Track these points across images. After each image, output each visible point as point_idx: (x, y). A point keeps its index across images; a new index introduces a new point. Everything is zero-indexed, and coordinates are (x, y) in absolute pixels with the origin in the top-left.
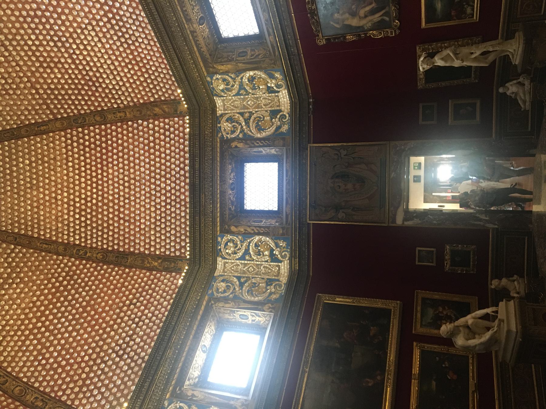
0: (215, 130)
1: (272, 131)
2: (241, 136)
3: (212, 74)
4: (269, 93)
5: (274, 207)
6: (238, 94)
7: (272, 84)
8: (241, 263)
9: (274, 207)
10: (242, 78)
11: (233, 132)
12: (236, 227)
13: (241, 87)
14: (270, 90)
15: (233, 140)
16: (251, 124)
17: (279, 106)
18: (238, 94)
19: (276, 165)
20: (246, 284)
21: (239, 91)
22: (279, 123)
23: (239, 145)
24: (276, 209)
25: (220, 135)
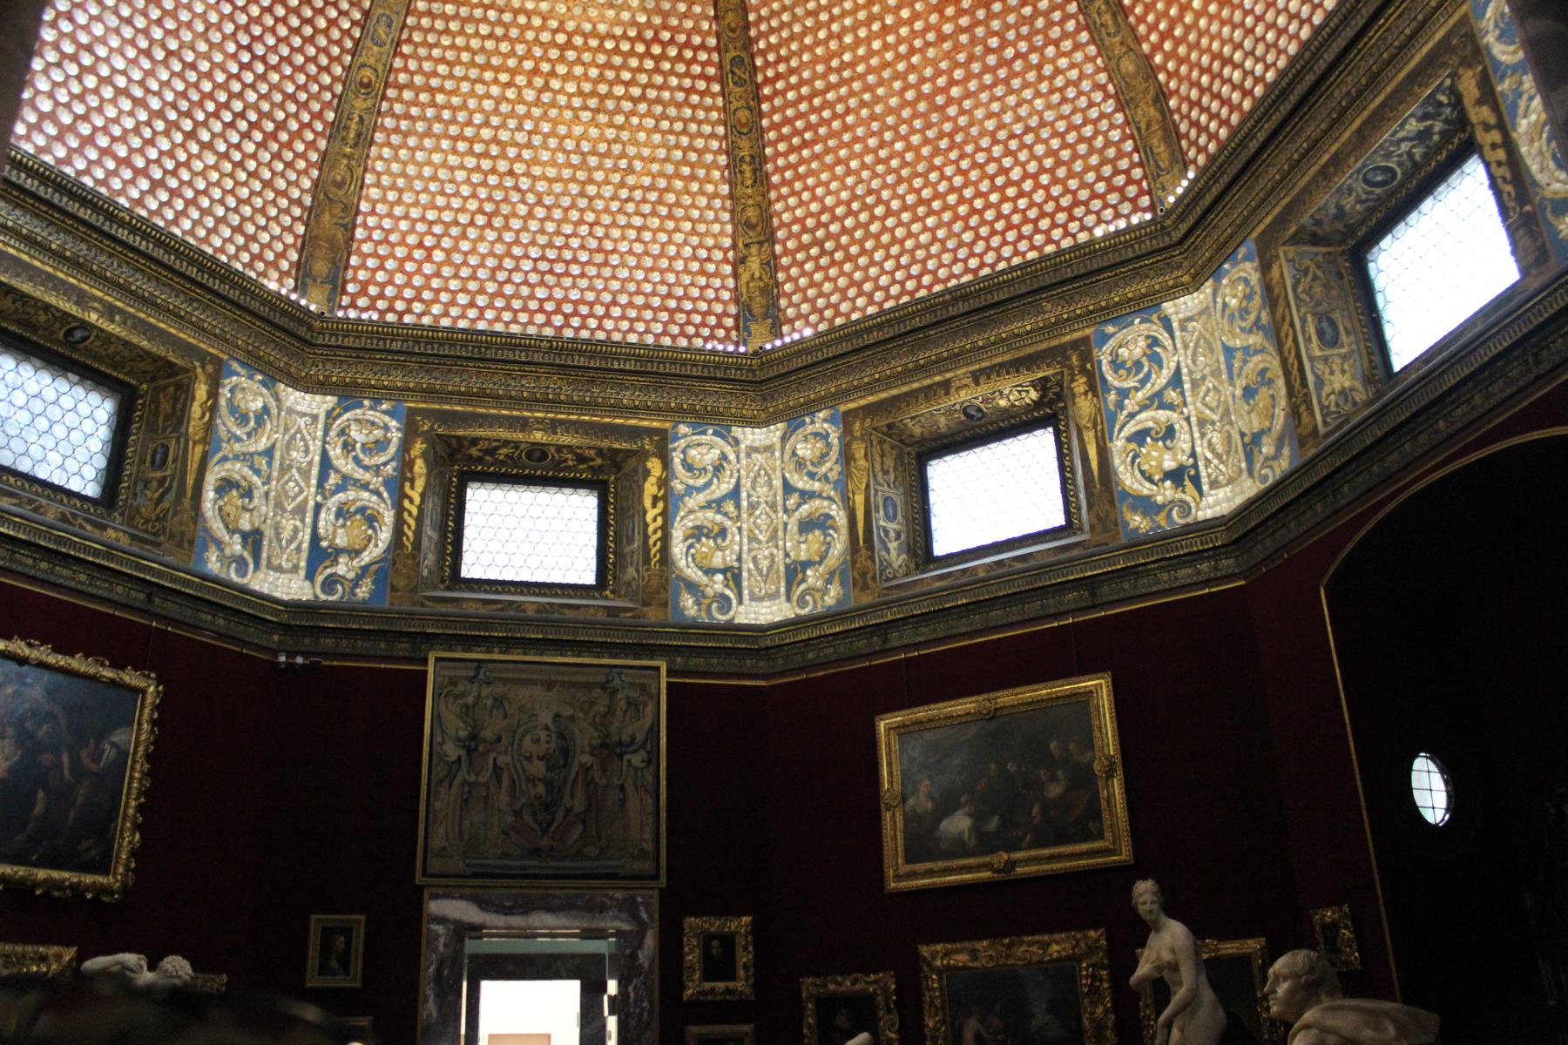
0: (702, 418)
1: (688, 572)
2: (678, 486)
3: (847, 420)
4: (787, 566)
5: (472, 568)
6: (788, 488)
7: (813, 577)
8: (310, 463)
9: (472, 568)
10: (829, 498)
11: (689, 467)
12: (424, 455)
13: (807, 496)
14: (795, 572)
15: (666, 464)
16: (710, 514)
17: (753, 598)
18: (788, 488)
19: (589, 578)
20: (247, 471)
21: (795, 490)
22: (710, 592)
23: (652, 480)
24: (464, 573)
25: (683, 429)
